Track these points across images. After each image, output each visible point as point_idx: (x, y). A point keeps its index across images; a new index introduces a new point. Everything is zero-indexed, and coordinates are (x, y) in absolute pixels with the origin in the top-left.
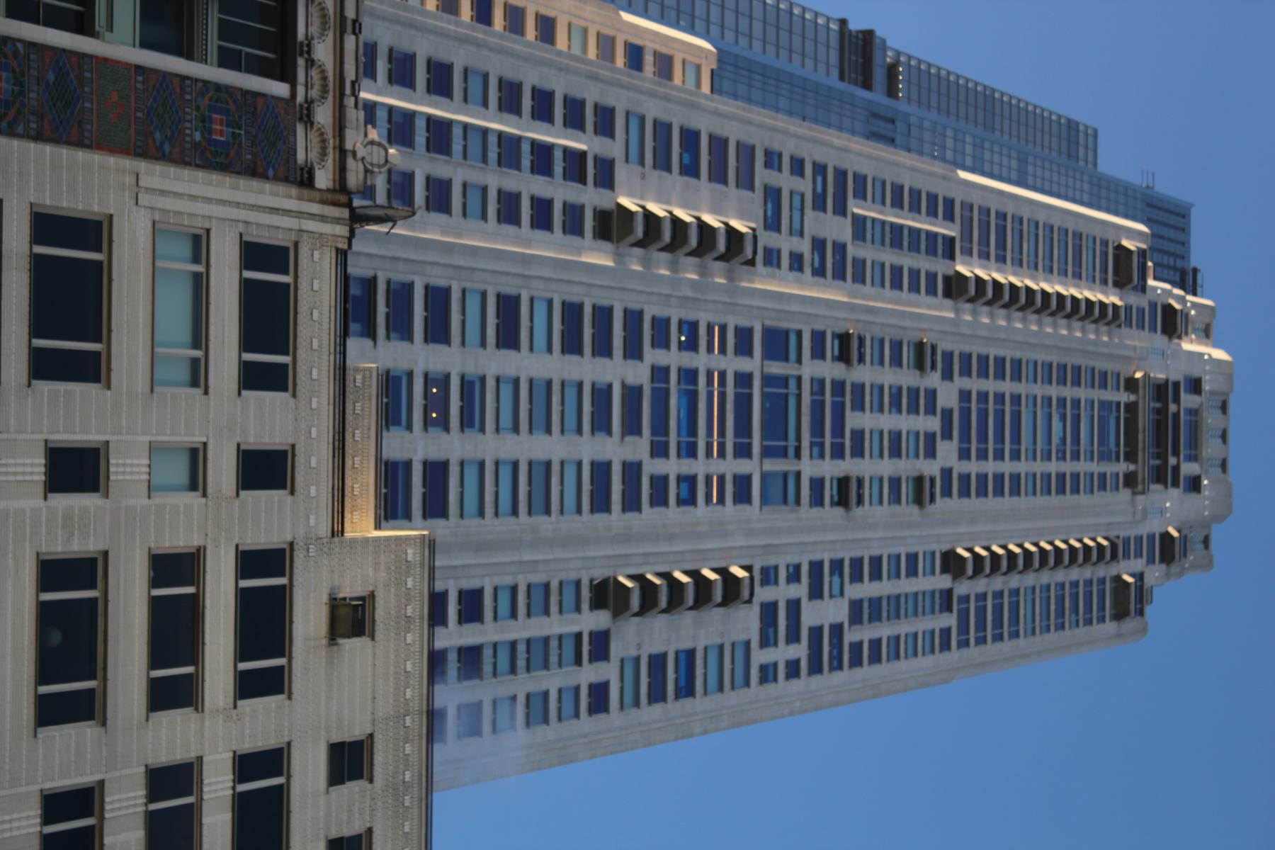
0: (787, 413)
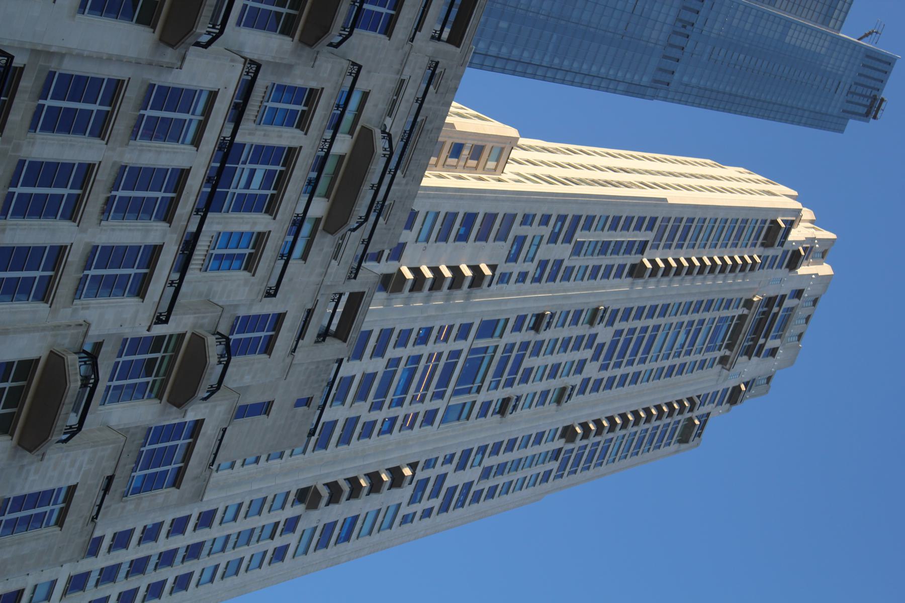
0: (479, 369)
